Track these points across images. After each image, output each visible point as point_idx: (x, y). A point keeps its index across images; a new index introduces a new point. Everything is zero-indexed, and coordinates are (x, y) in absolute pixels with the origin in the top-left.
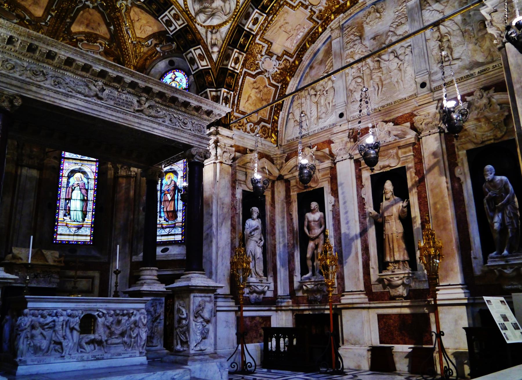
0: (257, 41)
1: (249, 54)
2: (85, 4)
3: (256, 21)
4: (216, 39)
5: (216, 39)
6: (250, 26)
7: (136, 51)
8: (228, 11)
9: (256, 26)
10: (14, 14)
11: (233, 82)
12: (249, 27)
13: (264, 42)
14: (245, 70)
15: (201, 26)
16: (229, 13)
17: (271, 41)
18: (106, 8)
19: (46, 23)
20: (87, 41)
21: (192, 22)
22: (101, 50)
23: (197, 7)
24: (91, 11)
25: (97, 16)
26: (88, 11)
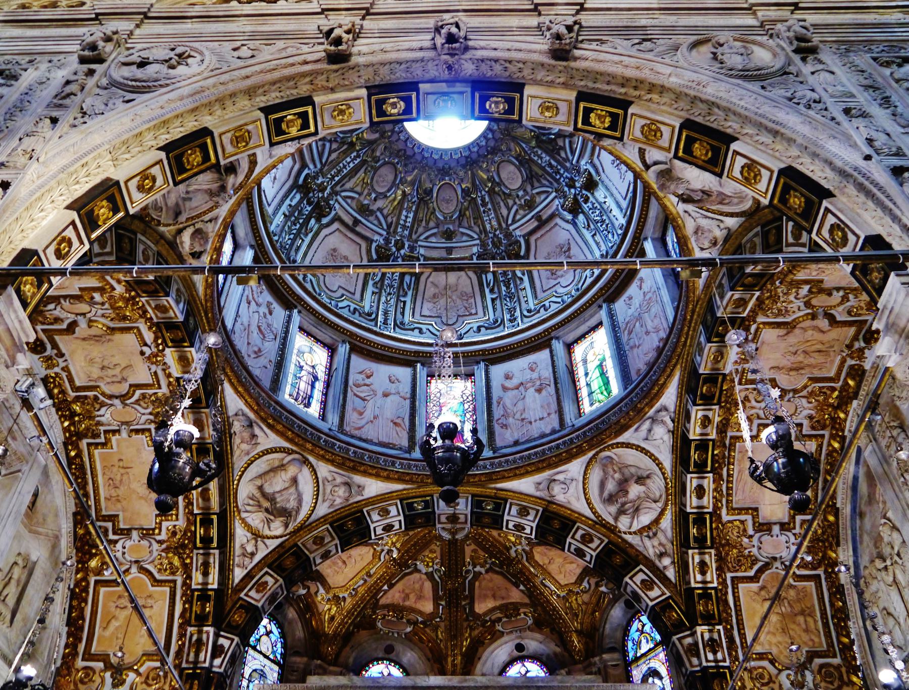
0: (725, 517)
1: (723, 546)
2: (474, 572)
3: (700, 491)
4: (660, 544)
5: (660, 544)
6: (695, 502)
7: (571, 608)
8: (658, 495)
9: (706, 499)
10: (404, 620)
11: (713, 607)
12: (694, 504)
13: (739, 514)
14: (729, 575)
15: (630, 533)
16: (661, 496)
17: (753, 506)
18: (501, 566)
19: (441, 618)
20: (507, 617)
21: (615, 534)
22: (530, 622)
23: (613, 509)
24: (487, 577)
25: (498, 580)
26: (484, 579)
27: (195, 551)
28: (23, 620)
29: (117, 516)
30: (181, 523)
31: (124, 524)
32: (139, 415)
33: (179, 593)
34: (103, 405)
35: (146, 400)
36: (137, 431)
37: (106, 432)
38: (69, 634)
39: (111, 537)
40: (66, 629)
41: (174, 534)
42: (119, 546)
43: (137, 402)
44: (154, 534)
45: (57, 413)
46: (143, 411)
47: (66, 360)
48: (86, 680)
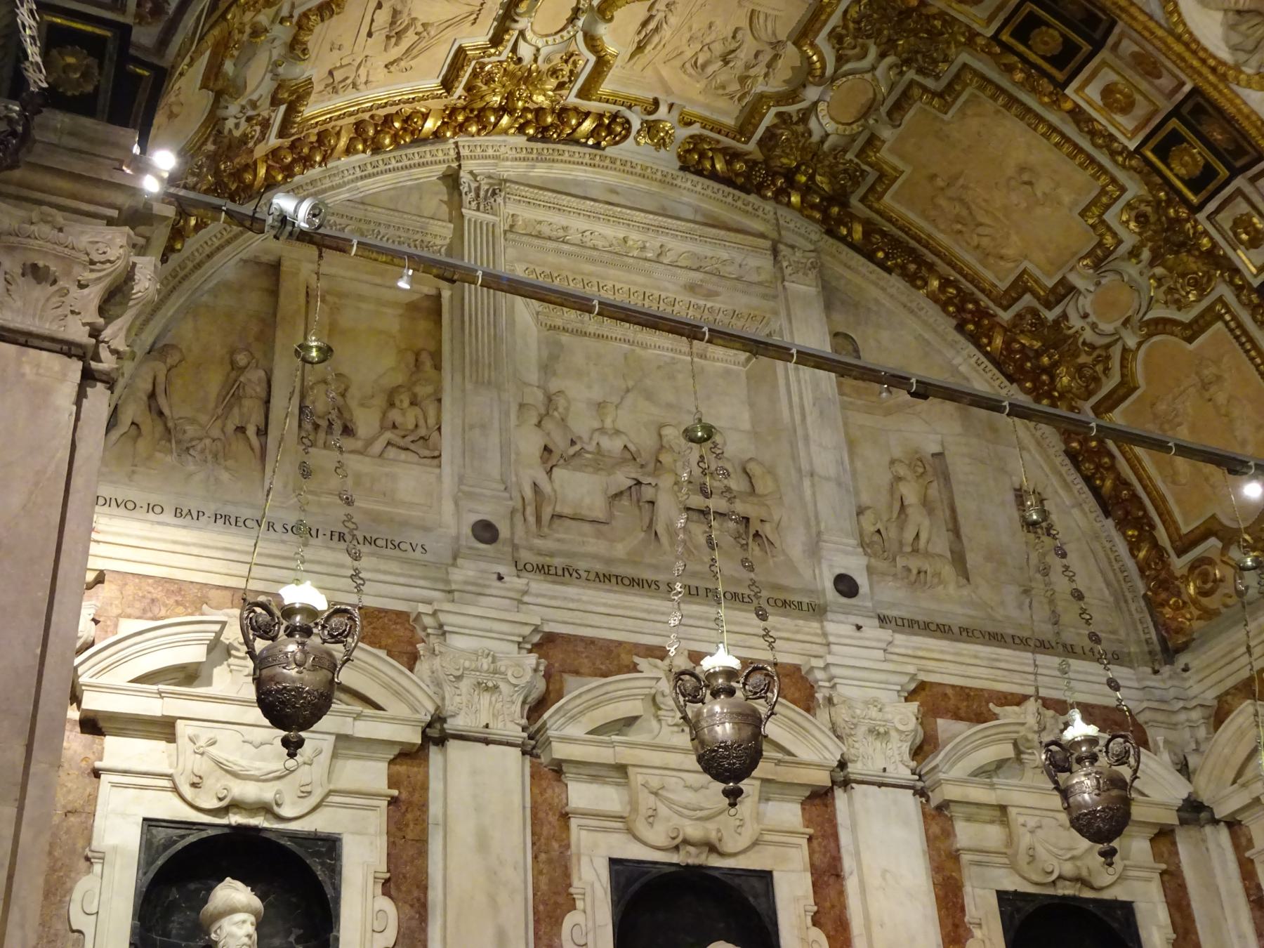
27: (1201, 216)
28: (989, 558)
29: (1025, 271)
30: (1134, 188)
31: (1049, 275)
32: (868, 76)
33: (1245, 317)
34: (805, 116)
35: (848, 40)
36: (899, 107)
37: (861, 154)
38: (1121, 525)
39: (1050, 315)
40: (1110, 523)
41: (1141, 219)
42: (1075, 322)
43: (841, 60)
44: (1108, 253)
45: (764, 197)
46: (866, 63)
47: (671, 106)
48: (1209, 585)
